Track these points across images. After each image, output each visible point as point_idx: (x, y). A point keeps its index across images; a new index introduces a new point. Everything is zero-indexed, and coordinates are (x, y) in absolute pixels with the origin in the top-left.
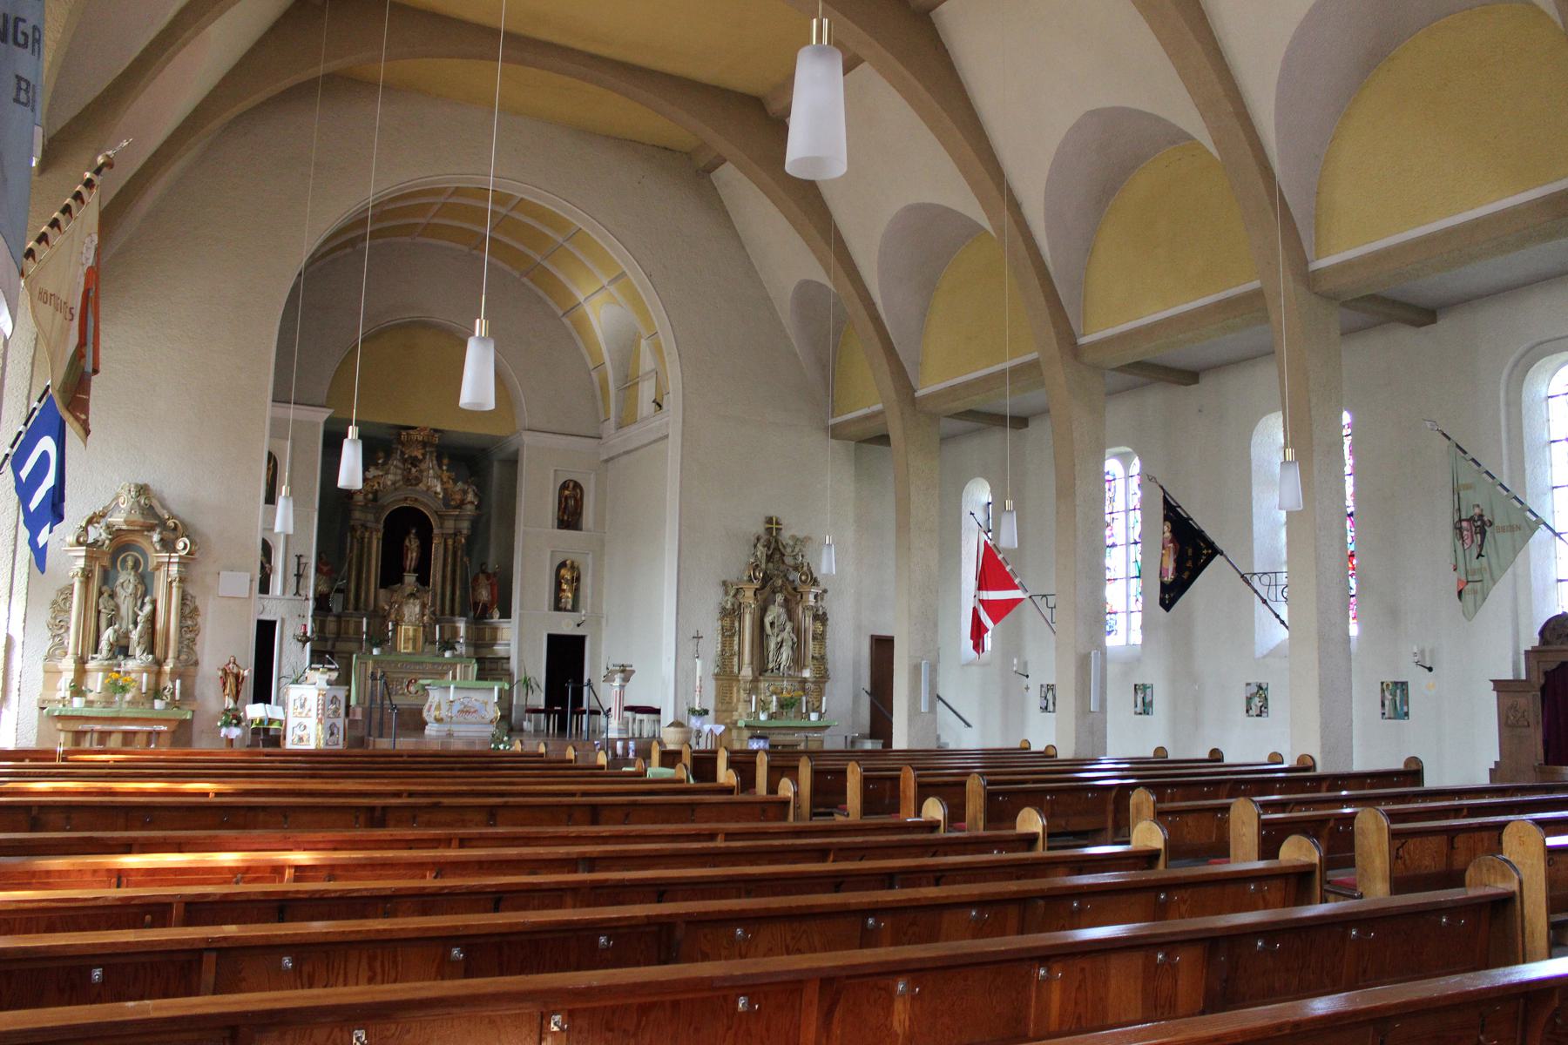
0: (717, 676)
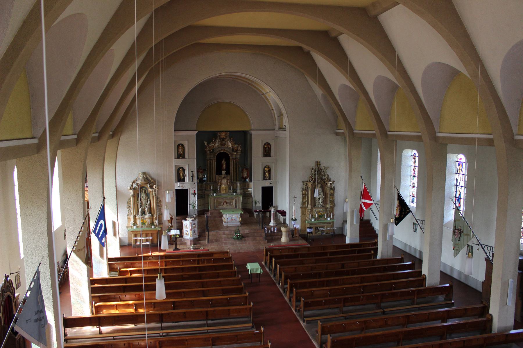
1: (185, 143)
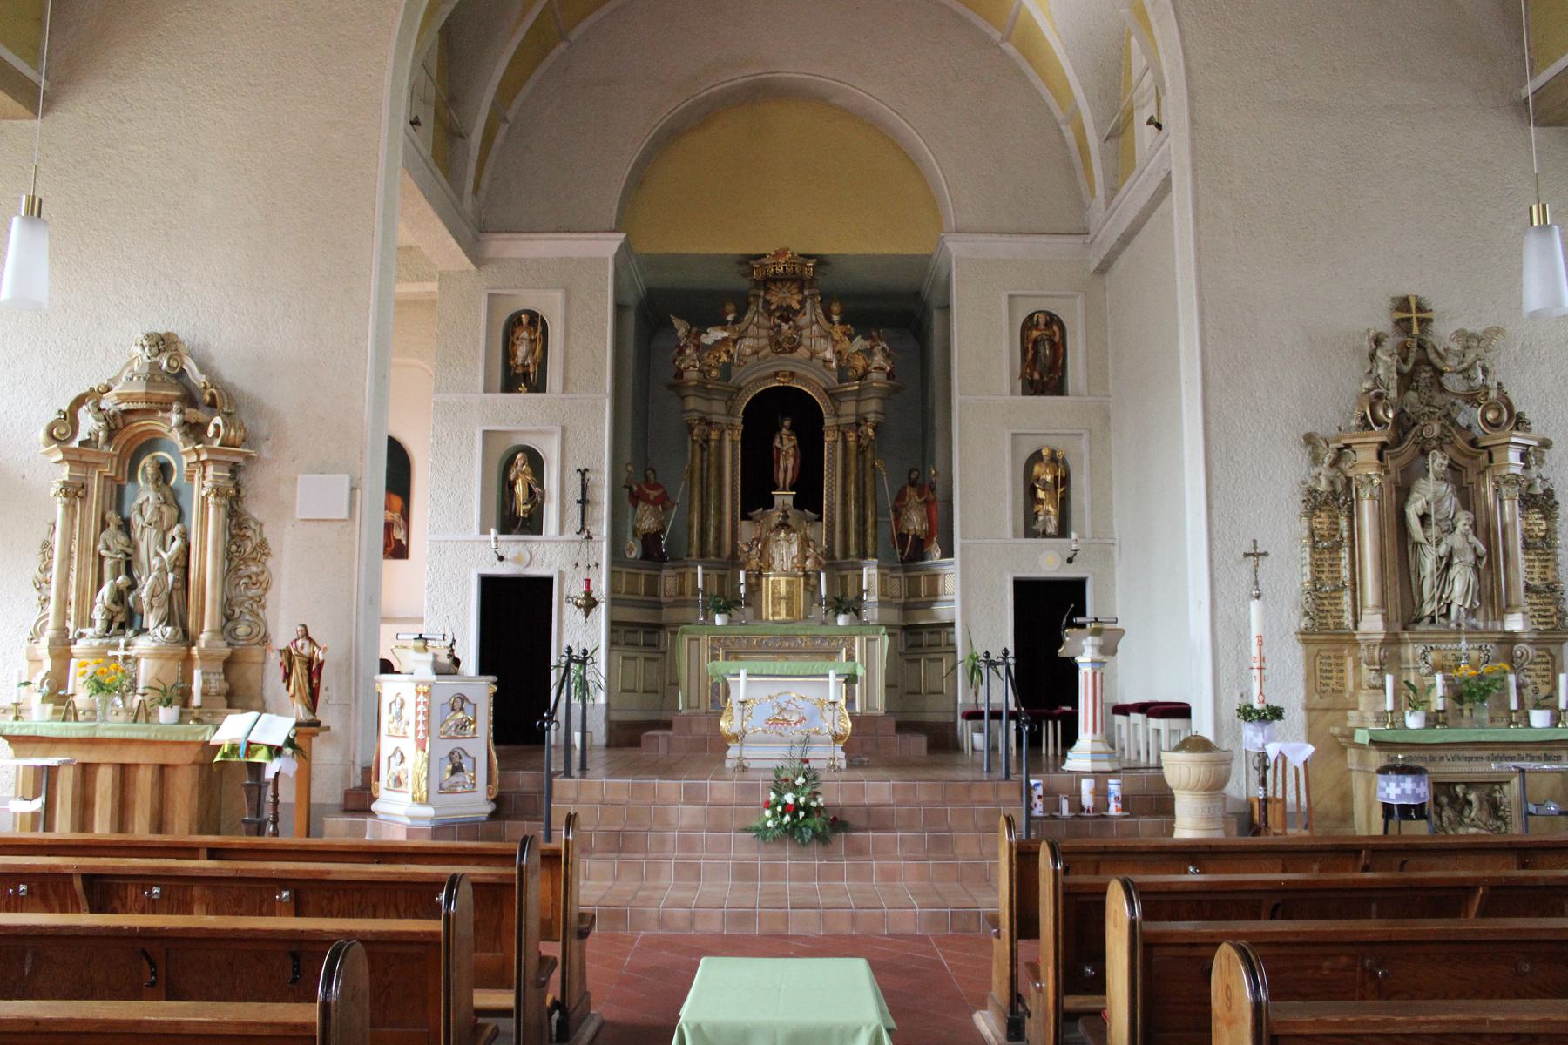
0: (1306, 636)
1: (550, 304)
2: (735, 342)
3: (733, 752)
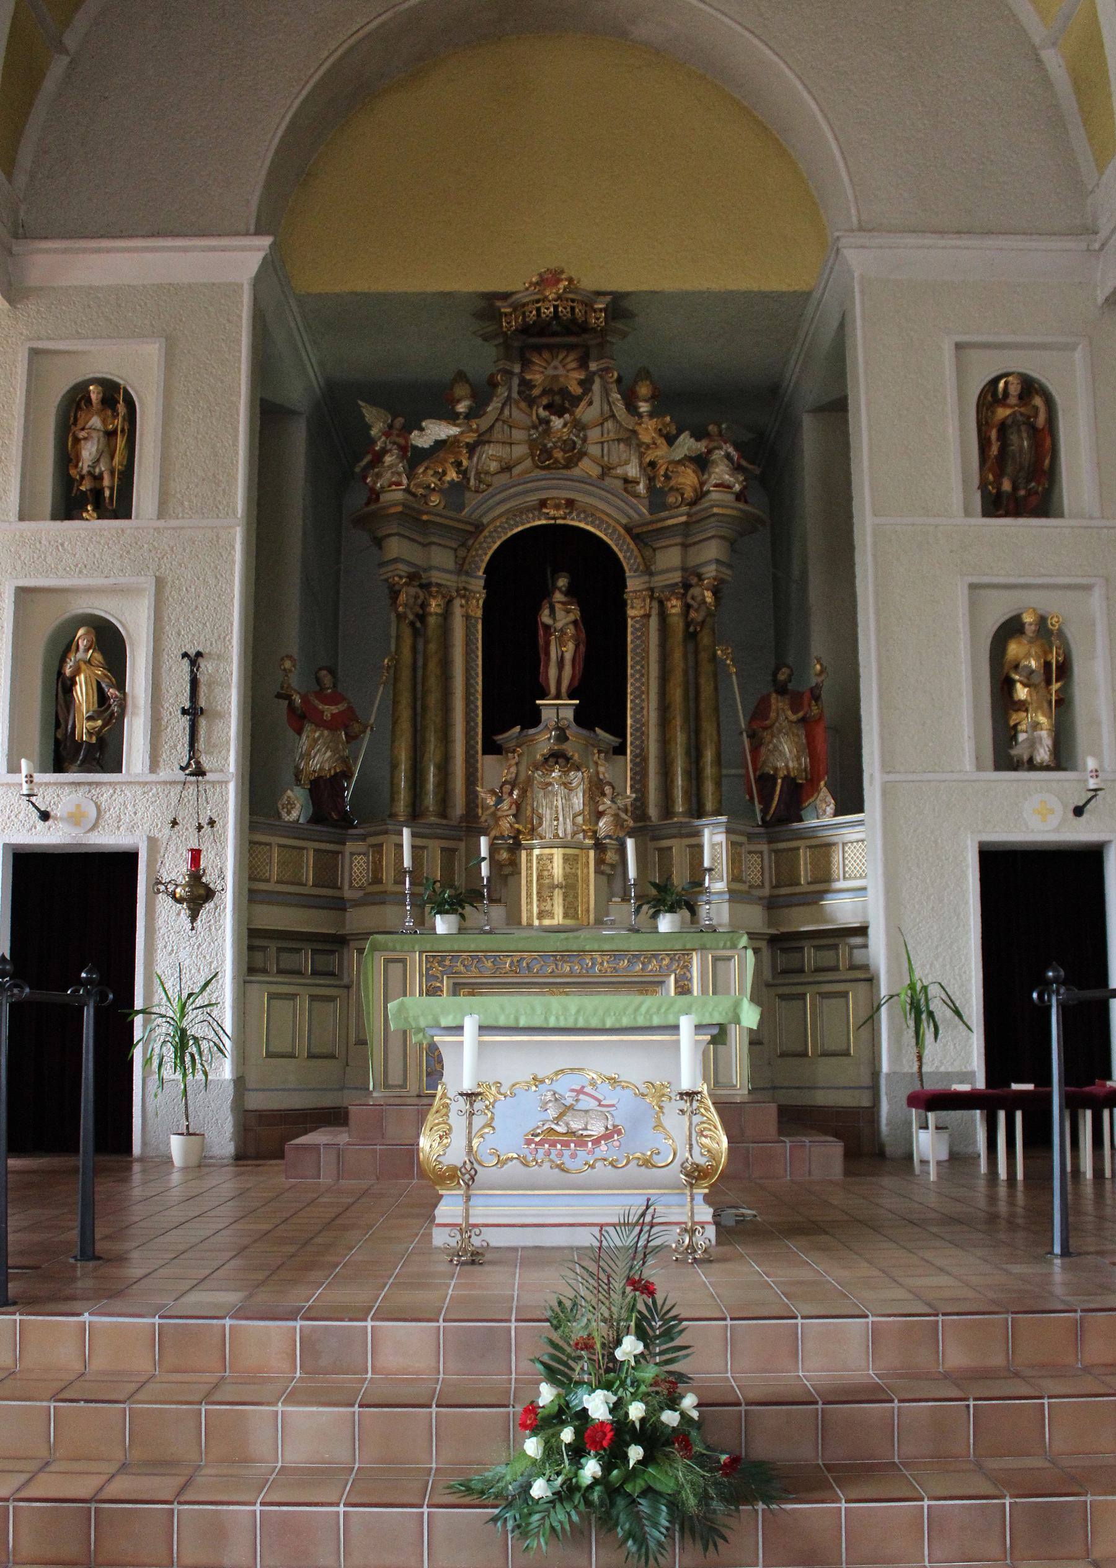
1: (138, 365)
2: (472, 448)
3: (449, 1209)
